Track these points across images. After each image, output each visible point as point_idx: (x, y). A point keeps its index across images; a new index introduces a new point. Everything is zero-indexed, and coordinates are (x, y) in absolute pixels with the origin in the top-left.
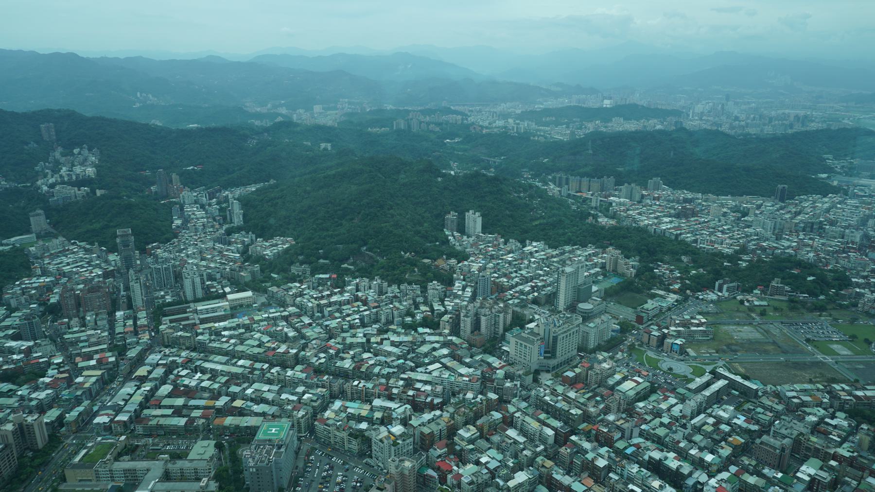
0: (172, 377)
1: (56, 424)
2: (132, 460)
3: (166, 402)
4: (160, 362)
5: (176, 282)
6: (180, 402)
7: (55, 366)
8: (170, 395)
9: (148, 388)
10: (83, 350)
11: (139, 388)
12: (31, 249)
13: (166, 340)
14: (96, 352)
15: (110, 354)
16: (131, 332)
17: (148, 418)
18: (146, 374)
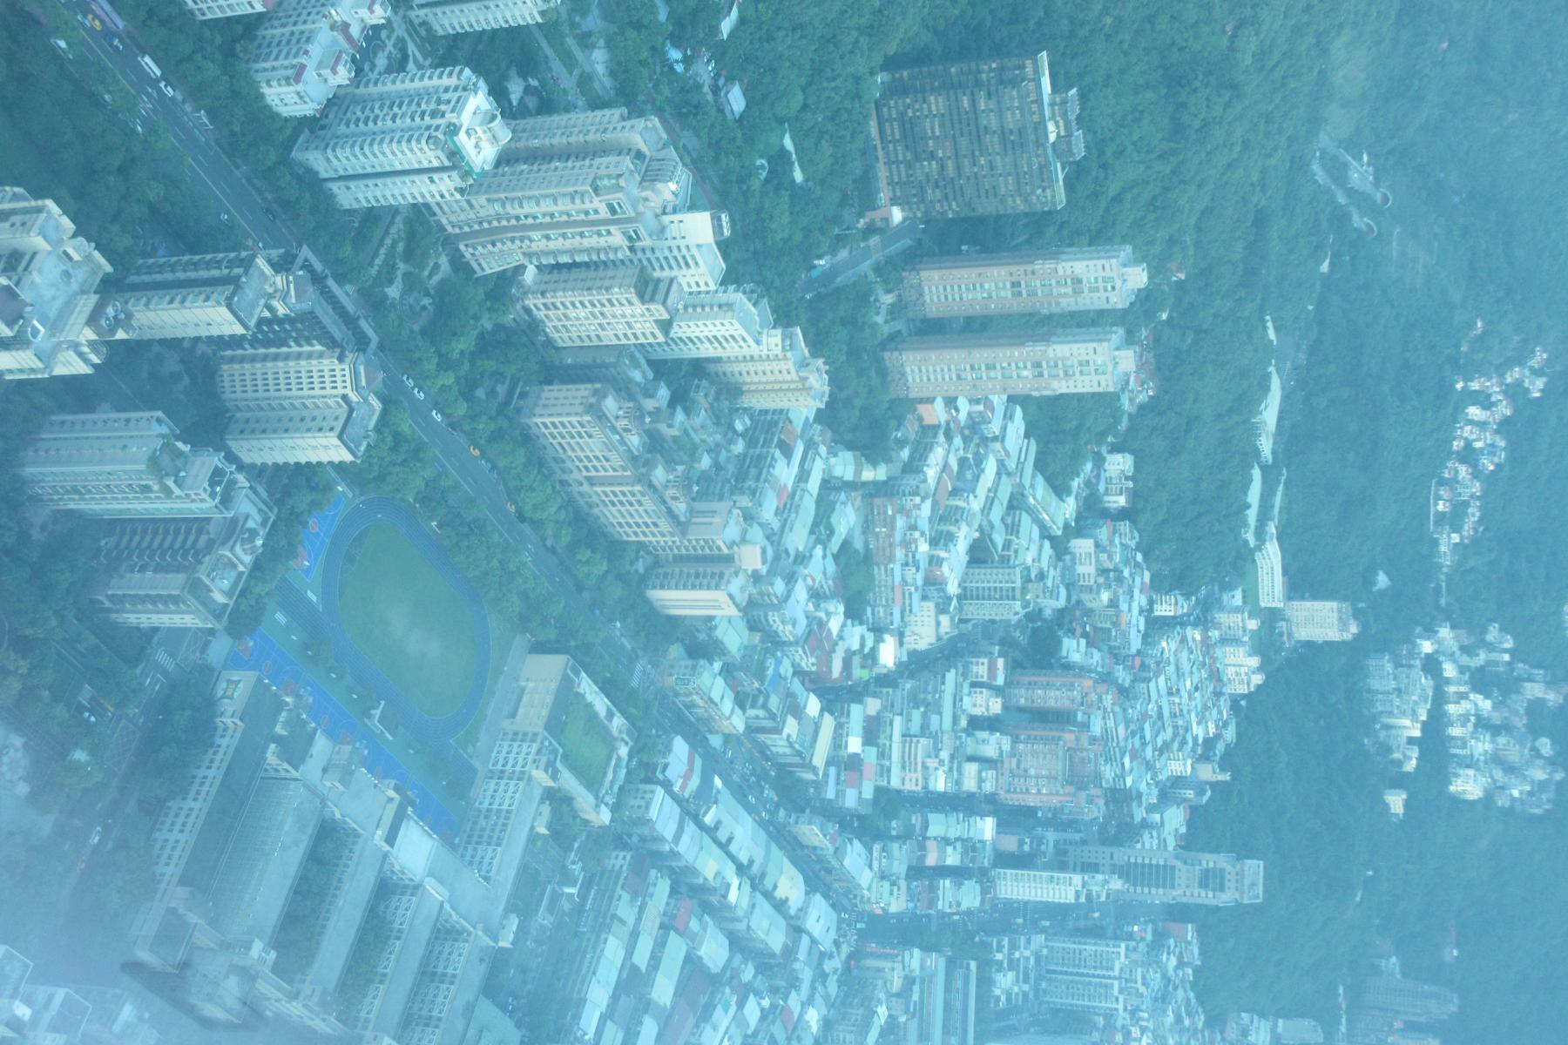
0: (748, 973)
1: (702, 637)
2: (533, 837)
3: (676, 948)
4: (805, 940)
5: (1055, 1012)
6: (663, 990)
7: (869, 643)
8: (692, 961)
9: (733, 897)
10: (898, 720)
11: (741, 869)
12: (1237, 598)
13: (870, 962)
14: (883, 754)
15: (868, 794)
16: (922, 858)
17: (640, 892)
18: (779, 894)
